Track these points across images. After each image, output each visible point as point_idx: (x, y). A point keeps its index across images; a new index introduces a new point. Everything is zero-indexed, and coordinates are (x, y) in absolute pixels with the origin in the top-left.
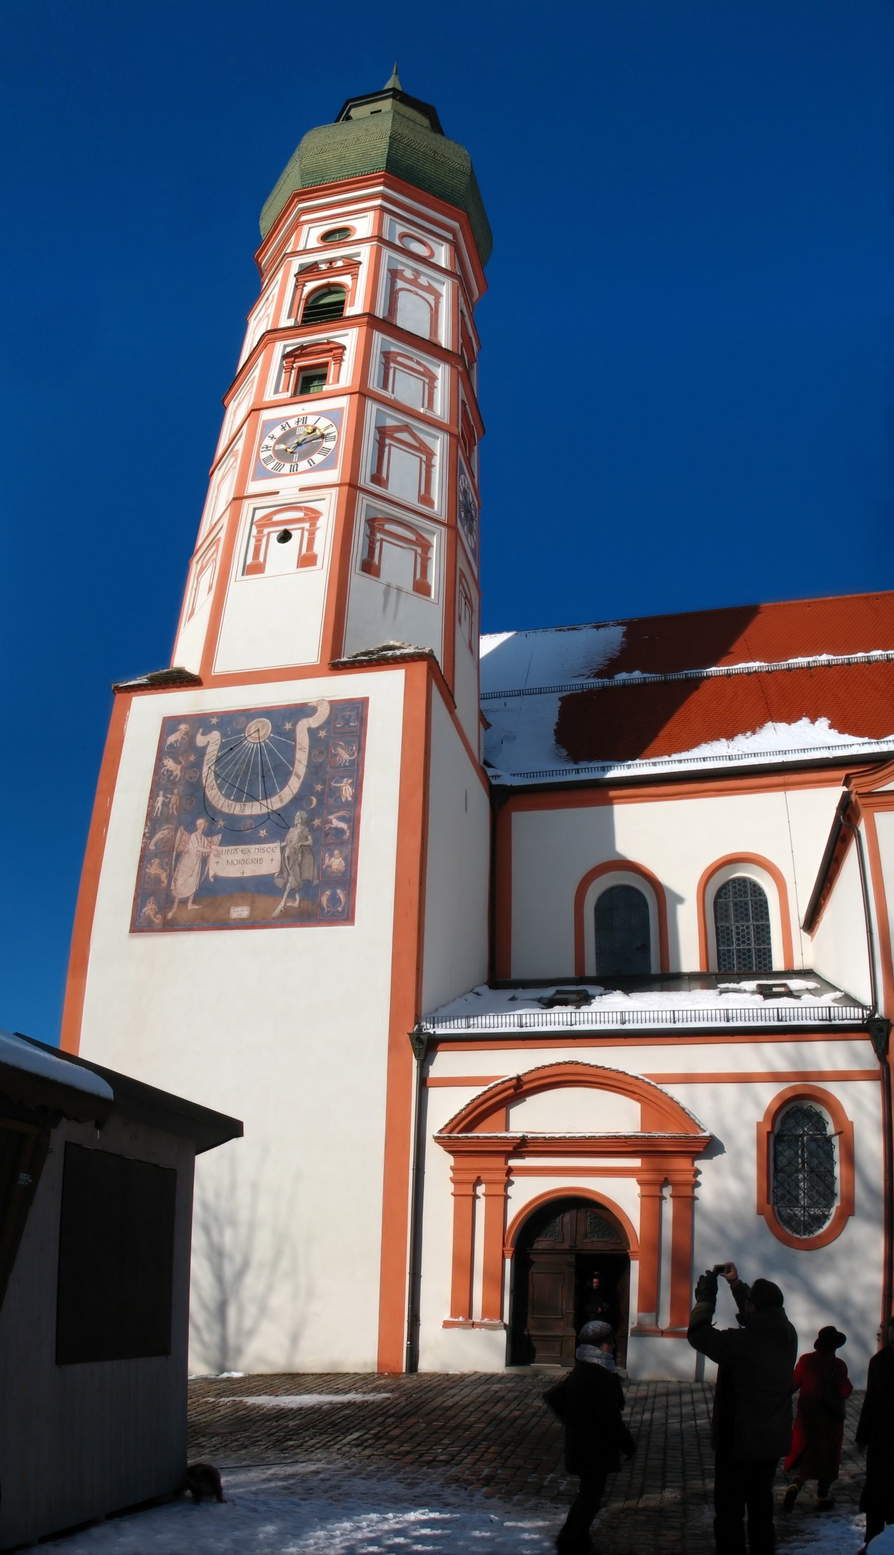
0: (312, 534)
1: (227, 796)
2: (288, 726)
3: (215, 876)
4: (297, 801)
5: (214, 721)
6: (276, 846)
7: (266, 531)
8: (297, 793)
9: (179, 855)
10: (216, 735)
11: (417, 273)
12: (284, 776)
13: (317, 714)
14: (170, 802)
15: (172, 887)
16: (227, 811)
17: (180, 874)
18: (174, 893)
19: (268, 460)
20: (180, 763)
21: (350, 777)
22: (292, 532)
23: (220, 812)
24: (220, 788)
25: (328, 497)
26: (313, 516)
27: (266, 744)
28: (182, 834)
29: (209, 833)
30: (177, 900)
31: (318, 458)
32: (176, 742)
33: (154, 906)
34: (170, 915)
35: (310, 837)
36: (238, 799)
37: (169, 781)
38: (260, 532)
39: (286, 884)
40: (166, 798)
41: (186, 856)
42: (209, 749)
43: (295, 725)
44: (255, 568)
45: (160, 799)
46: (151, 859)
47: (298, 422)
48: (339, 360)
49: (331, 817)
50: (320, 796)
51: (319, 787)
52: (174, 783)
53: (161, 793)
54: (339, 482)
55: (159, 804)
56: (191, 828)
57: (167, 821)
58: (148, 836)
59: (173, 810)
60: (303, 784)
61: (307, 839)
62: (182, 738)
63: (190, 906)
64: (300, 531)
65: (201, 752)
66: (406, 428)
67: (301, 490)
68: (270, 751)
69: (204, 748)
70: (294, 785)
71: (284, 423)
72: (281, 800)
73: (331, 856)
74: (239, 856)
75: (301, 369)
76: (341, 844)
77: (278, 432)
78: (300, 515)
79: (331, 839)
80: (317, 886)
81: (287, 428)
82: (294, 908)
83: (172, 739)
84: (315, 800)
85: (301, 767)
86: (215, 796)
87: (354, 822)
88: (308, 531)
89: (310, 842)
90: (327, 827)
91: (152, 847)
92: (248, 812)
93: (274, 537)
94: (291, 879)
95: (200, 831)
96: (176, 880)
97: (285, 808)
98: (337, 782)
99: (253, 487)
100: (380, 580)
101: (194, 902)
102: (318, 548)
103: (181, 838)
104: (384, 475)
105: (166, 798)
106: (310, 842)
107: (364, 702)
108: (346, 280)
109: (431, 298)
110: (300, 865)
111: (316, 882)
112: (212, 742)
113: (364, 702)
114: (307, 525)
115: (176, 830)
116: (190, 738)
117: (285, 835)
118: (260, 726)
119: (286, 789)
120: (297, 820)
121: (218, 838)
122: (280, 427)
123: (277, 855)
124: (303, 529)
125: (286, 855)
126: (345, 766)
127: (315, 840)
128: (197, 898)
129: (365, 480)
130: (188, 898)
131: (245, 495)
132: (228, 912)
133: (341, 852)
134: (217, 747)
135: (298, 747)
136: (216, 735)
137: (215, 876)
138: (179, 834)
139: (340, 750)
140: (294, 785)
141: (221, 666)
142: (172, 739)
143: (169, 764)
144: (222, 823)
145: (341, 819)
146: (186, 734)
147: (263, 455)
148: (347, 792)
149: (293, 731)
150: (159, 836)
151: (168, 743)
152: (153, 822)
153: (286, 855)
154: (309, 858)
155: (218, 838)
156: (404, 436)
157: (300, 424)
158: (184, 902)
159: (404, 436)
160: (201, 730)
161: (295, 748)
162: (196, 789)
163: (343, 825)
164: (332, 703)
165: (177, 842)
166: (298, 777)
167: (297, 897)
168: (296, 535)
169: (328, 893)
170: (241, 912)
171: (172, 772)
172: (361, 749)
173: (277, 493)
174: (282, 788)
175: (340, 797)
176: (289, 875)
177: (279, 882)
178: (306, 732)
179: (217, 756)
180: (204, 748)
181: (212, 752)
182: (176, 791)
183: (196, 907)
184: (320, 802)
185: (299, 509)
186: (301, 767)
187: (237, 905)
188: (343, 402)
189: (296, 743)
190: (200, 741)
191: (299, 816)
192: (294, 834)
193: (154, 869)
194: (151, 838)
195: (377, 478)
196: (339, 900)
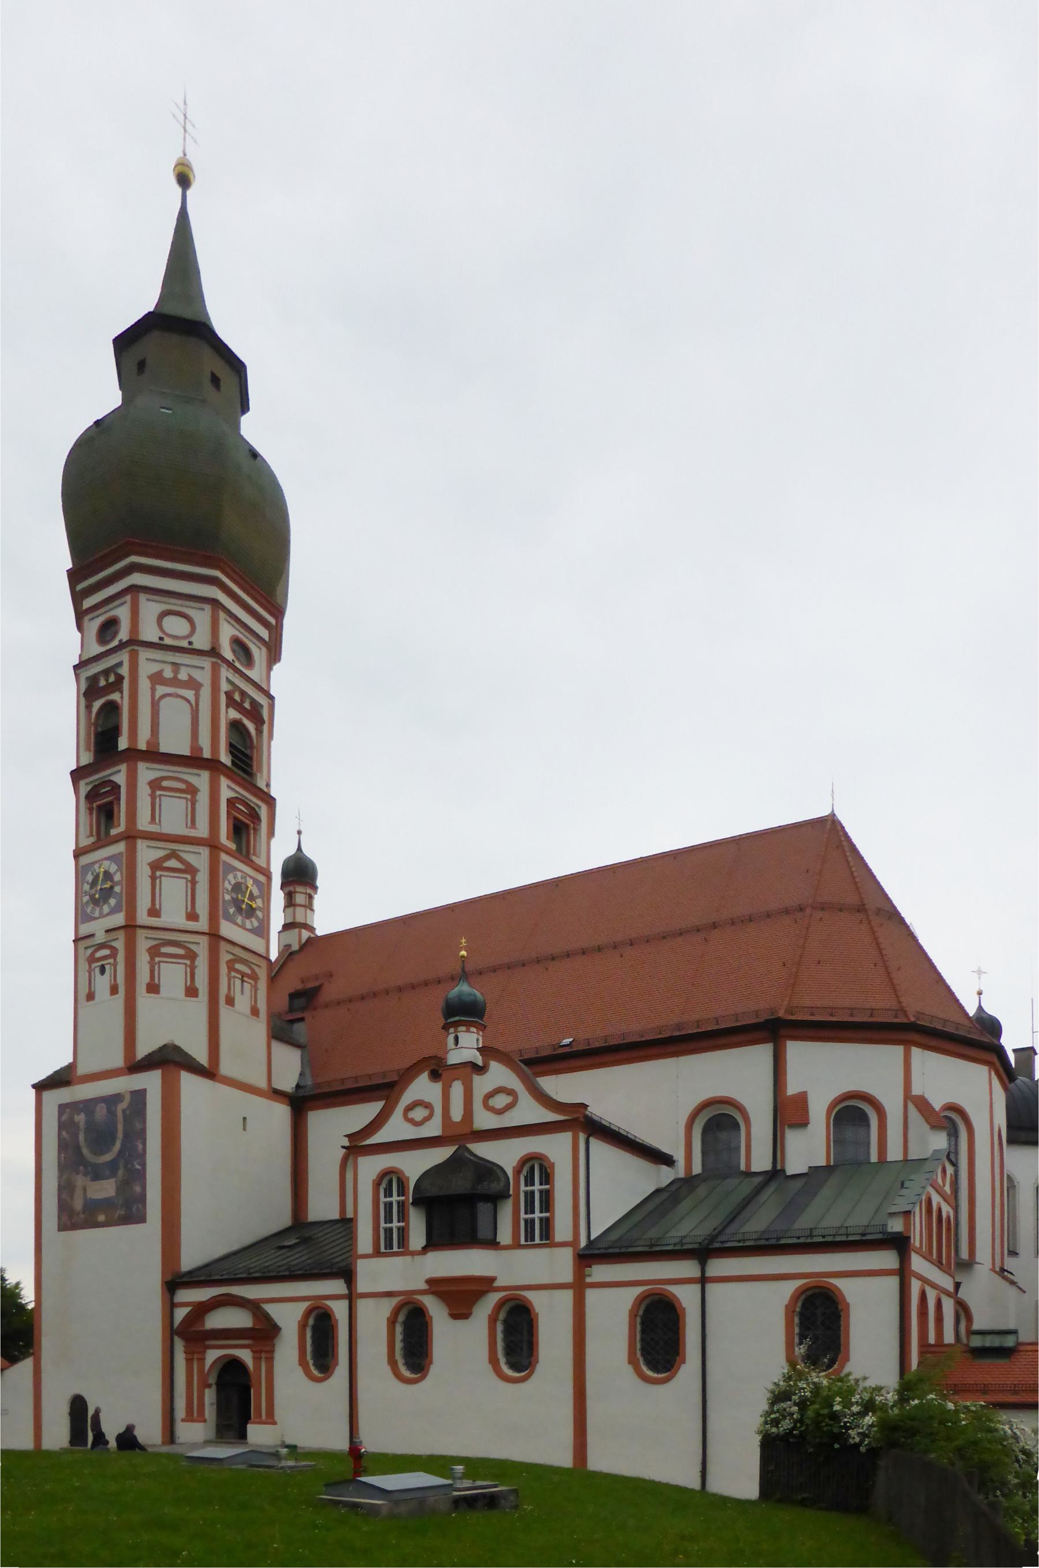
3: (90, 1198)
5: (81, 1106)
11: (176, 666)
25: (119, 937)
26: (114, 952)
29: (85, 1175)
31: (112, 902)
34: (74, 1221)
48: (118, 799)
54: (124, 924)
65: (76, 1125)
66: (173, 855)
67: (107, 931)
70: (118, 1145)
85: (120, 1135)
86: (85, 1151)
93: (97, 970)
104: (157, 906)
109: (189, 694)
112: (81, 1118)
114: (111, 961)
120: (121, 1165)
128: (84, 1212)
129: (142, 917)
140: (118, 1145)
150: (64, 1177)
155: (89, 1178)
156: (173, 863)
159: (173, 863)
162: (78, 1149)
164: (132, 1093)
168: (107, 967)
170: (101, 1218)
181: (82, 1125)
186: (120, 1135)
193: (63, 1196)
195: (154, 912)
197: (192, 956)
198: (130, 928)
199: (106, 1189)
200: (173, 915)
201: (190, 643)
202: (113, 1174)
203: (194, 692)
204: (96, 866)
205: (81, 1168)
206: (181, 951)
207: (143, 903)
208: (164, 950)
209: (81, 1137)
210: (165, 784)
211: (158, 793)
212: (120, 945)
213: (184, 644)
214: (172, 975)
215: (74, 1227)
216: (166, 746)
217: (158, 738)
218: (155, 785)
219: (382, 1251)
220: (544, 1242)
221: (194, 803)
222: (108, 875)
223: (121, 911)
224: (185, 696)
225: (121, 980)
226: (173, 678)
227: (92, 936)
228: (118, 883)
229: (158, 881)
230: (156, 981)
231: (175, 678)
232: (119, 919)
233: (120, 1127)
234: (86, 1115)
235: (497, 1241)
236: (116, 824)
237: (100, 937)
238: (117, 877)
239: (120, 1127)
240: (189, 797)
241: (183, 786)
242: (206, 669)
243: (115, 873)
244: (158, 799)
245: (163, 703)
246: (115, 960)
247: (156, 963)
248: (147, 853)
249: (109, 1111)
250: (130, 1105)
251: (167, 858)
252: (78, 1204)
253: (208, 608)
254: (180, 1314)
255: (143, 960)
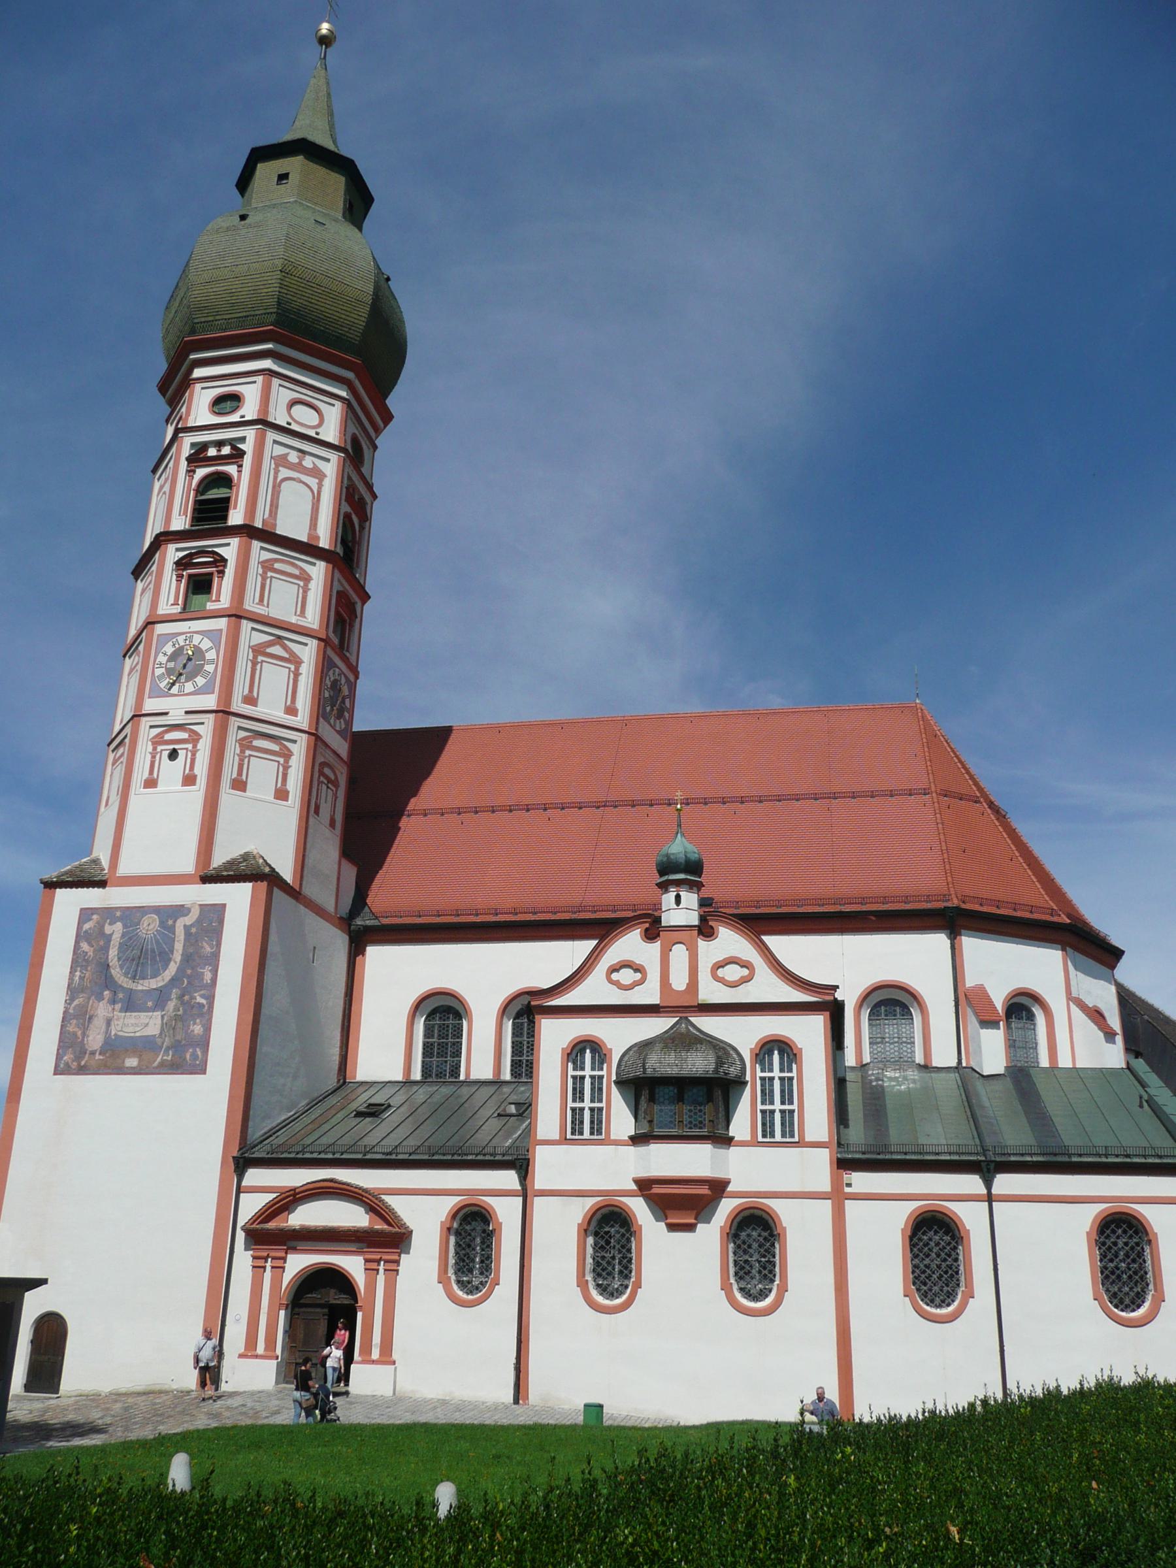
0: (194, 754)
1: (126, 975)
2: (170, 922)
4: (174, 981)
5: (118, 914)
6: (158, 1014)
7: (159, 748)
8: (175, 975)
9: (91, 1018)
10: (119, 925)
12: (166, 962)
13: (190, 914)
14: (84, 977)
15: (85, 1042)
16: (125, 986)
17: (91, 1032)
18: (87, 1047)
19: (161, 677)
20: (93, 946)
21: (210, 965)
22: (179, 751)
23: (121, 986)
24: (121, 967)
26: (195, 738)
27: (155, 935)
28: (94, 1002)
29: (113, 1002)
30: (88, 1052)
31: (200, 681)
32: (90, 929)
33: (72, 1056)
35: (181, 1009)
36: (134, 978)
37: (84, 960)
38: (155, 749)
39: (163, 1043)
40: (83, 973)
41: (96, 1019)
42: (114, 937)
43: (175, 922)
44: (151, 783)
45: (78, 974)
46: (71, 1019)
47: (186, 640)
48: (222, 573)
49: (196, 995)
50: (189, 977)
51: (189, 972)
52: (87, 961)
53: (79, 969)
54: (215, 708)
55: (77, 978)
56: (100, 998)
57: (82, 991)
58: (69, 1002)
59: (87, 983)
60: (178, 969)
61: (179, 1011)
62: (95, 926)
63: (97, 1057)
64: (185, 751)
67: (187, 712)
68: (157, 942)
69: (111, 935)
70: (172, 969)
71: (174, 640)
72: (163, 980)
73: (195, 1024)
74: (133, 1021)
75: (190, 576)
76: (201, 1015)
77: (169, 649)
78: (184, 735)
79: (195, 1011)
80: (185, 1045)
81: (177, 646)
82: (167, 1060)
83: (87, 926)
84: (186, 981)
85: (177, 956)
86: (116, 972)
87: (211, 998)
88: (191, 751)
89: (181, 1012)
90: (193, 1001)
91: (71, 1011)
92: (140, 988)
93: (166, 754)
94: (167, 1039)
95: (106, 1000)
96: (88, 1036)
97: (165, 986)
98: (201, 968)
99: (150, 705)
100: (248, 794)
101: (100, 1054)
102: (197, 771)
103: (92, 1005)
104: (255, 694)
105: (83, 973)
106: (181, 1012)
107: (224, 905)
108: (231, 469)
109: (313, 482)
110: (174, 1029)
111: (183, 1042)
112: (116, 930)
113: (224, 905)
114: (190, 746)
115: (89, 999)
116: (100, 926)
117: (165, 1006)
118: (151, 921)
119: (167, 971)
120: (173, 996)
121: (118, 1006)
122: (171, 643)
123: (159, 1022)
124: (187, 749)
125: (165, 1021)
126: (207, 956)
127: (185, 1011)
130: (96, 1050)
131: (144, 712)
132: (123, 1062)
133: (201, 1021)
134: (120, 935)
135: (176, 939)
136: (119, 925)
137: (115, 1035)
138: (91, 1002)
139: (205, 944)
140: (172, 969)
141: (124, 869)
142: (87, 926)
143: (85, 946)
144: (121, 995)
145: (202, 996)
146: (98, 923)
147: (159, 672)
148: (208, 976)
149: (174, 926)
150: (76, 1002)
151: (84, 930)
152: (73, 991)
153: (165, 1021)
154: (180, 1024)
155: (118, 1006)
157: (187, 642)
158: (93, 1053)
159: (276, 650)
160: (108, 921)
161: (174, 941)
163: (203, 1001)
165: (89, 1008)
166: (176, 963)
167: (171, 1052)
168: (182, 753)
169: (191, 1050)
170: (132, 1062)
171: (87, 953)
172: (219, 945)
173: (166, 714)
174: (164, 972)
175: (203, 979)
176: (166, 1036)
177: (159, 1041)
178: (182, 928)
179: (120, 943)
180: (111, 935)
181: (116, 939)
182: (89, 968)
183: (101, 1057)
184: (189, 983)
185: (185, 730)
187: (129, 1057)
188: (222, 623)
189: (175, 934)
190: (108, 929)
191: (175, 992)
192: (171, 1005)
194: (70, 1004)
196: (198, 1056)
197: (287, 755)
198: (224, 713)
199: (148, 1024)
200: (271, 706)
201: (317, 434)
202: (160, 1005)
203: (317, 481)
204: (181, 639)
205: (106, 993)
206: (276, 748)
207: (240, 688)
208: (258, 743)
209: (113, 953)
210: (277, 566)
211: (270, 574)
212: (206, 728)
213: (312, 433)
214: (263, 773)
215: (82, 1070)
216: (283, 529)
217: (275, 519)
218: (267, 566)
219: (568, 1137)
220: (768, 1140)
221: (306, 590)
222: (199, 652)
223: (213, 693)
224: (306, 481)
225: (202, 769)
226: (297, 463)
227: (166, 714)
228: (211, 662)
229: (258, 667)
230: (244, 777)
231: (300, 463)
232: (210, 701)
233: (179, 946)
234: (125, 926)
235: (731, 1134)
236: (214, 598)
237: (176, 717)
238: (211, 655)
239: (179, 946)
240: (301, 583)
241: (297, 572)
242: (331, 461)
243: (207, 651)
244: (268, 580)
245: (284, 485)
246: (195, 746)
247: (246, 757)
248: (250, 636)
249: (163, 924)
250: (199, 921)
251: (270, 644)
252: (95, 1040)
253: (338, 404)
254: (251, 1206)
255: (232, 749)
